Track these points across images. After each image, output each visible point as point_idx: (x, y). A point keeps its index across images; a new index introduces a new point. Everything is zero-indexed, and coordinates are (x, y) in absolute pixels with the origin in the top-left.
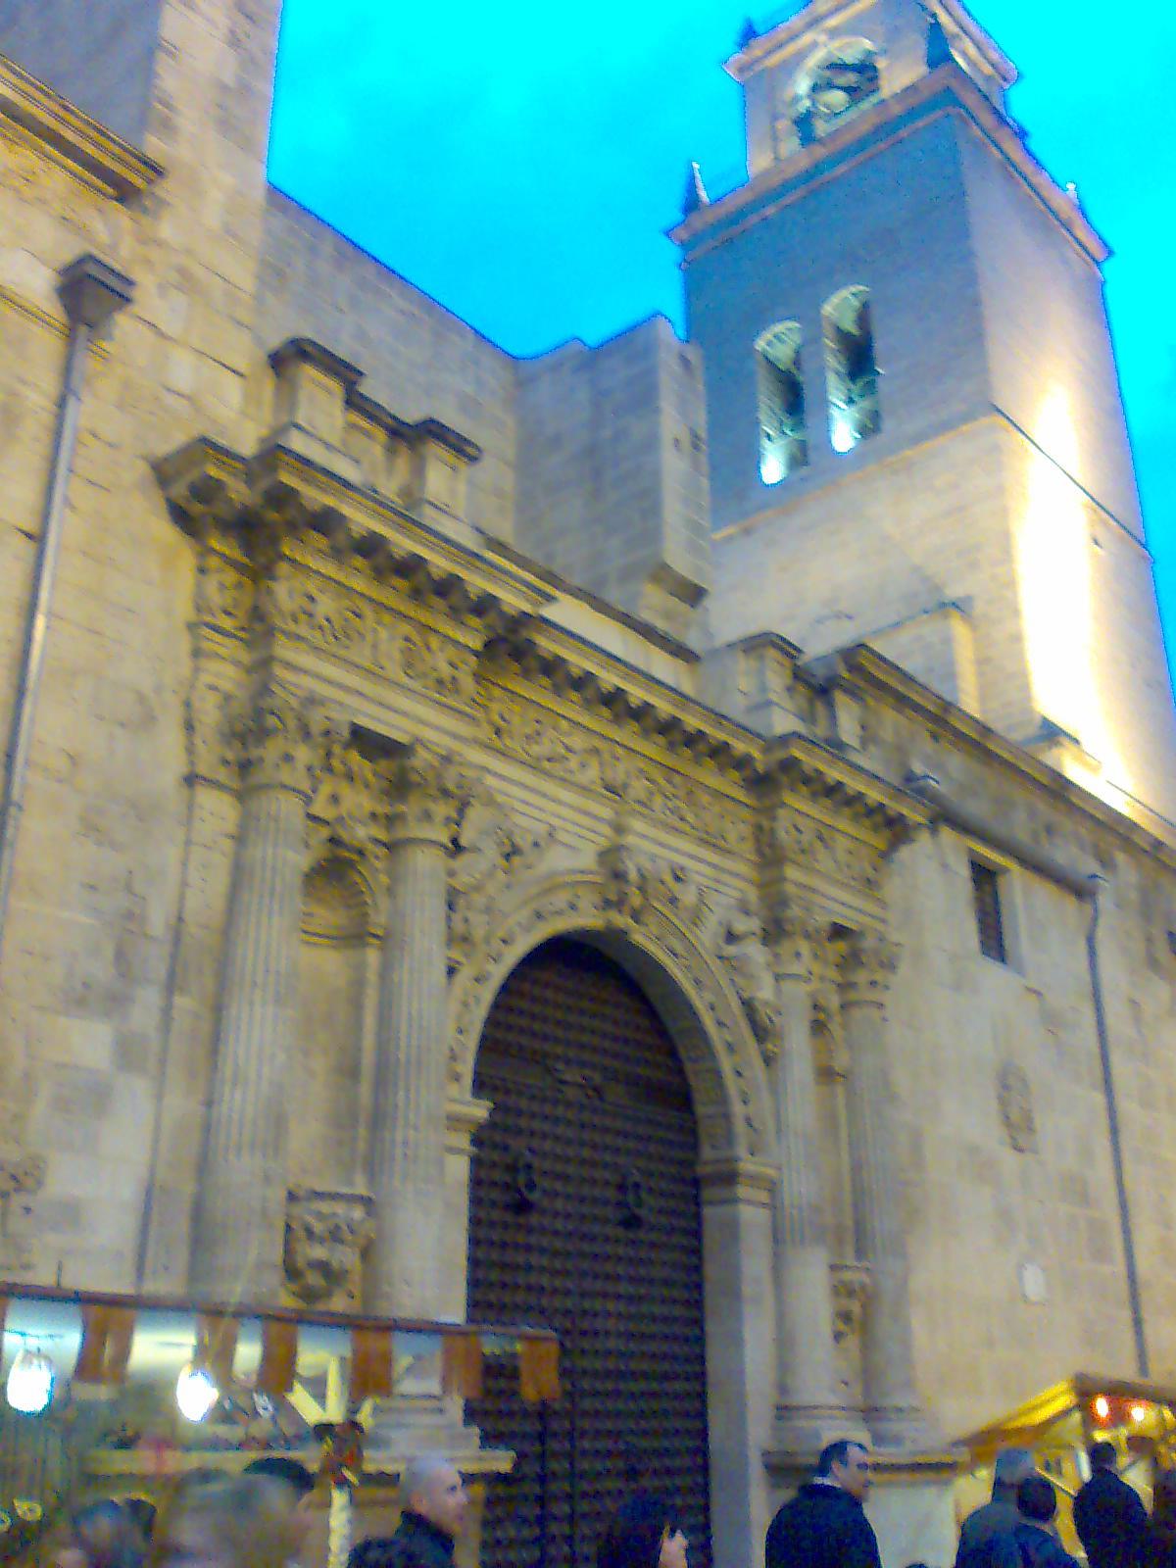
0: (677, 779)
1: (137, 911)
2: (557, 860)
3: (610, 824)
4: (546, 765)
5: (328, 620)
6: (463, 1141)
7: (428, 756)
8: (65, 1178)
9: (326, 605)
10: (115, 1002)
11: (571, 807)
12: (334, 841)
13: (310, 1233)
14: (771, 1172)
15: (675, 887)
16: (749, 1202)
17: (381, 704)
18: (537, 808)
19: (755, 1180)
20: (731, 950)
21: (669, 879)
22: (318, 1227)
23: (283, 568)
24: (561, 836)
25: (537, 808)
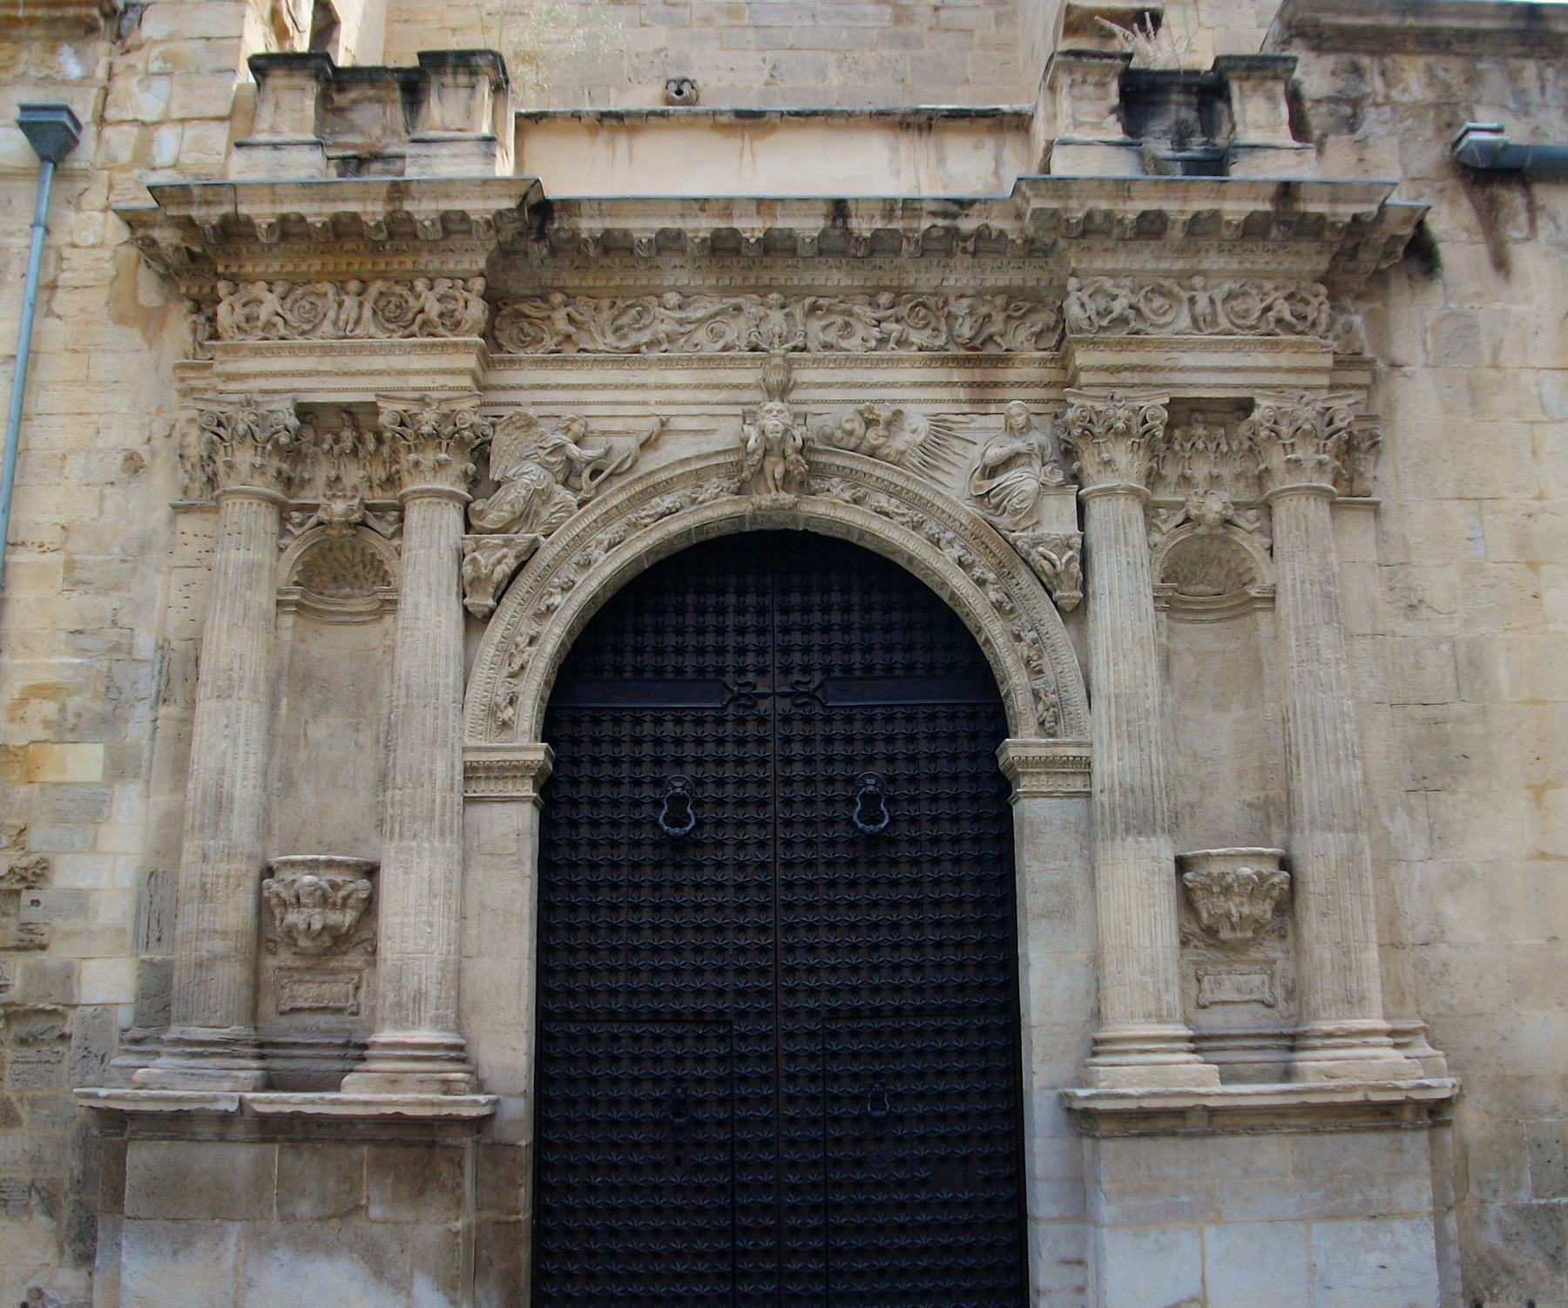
0: (884, 298)
1: (124, 641)
2: (674, 450)
3: (758, 386)
4: (656, 354)
5: (278, 314)
6: (528, 789)
7: (400, 407)
8: (68, 875)
9: (270, 303)
10: (107, 724)
11: (687, 387)
12: (320, 523)
13: (284, 904)
14: (1072, 752)
15: (873, 437)
16: (1034, 795)
17: (345, 374)
18: (638, 403)
19: (1049, 765)
20: (989, 485)
21: (857, 425)
22: (284, 895)
23: (223, 288)
24: (676, 424)
25: (638, 403)
